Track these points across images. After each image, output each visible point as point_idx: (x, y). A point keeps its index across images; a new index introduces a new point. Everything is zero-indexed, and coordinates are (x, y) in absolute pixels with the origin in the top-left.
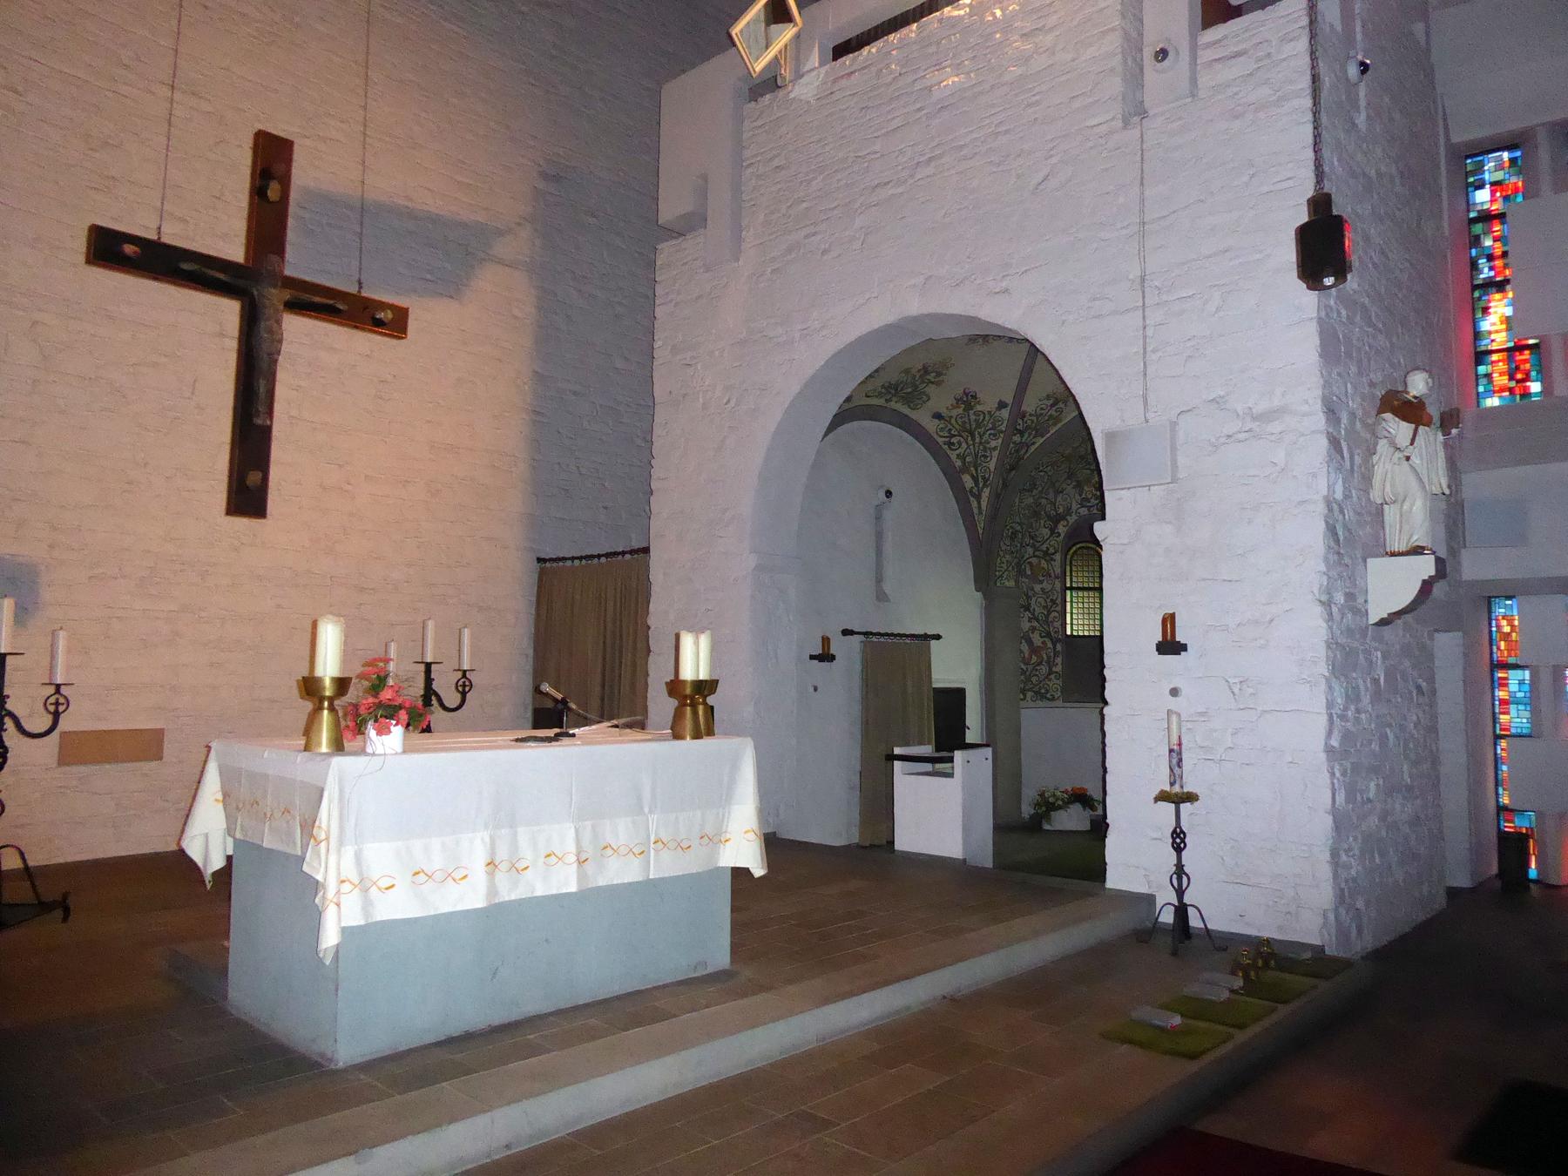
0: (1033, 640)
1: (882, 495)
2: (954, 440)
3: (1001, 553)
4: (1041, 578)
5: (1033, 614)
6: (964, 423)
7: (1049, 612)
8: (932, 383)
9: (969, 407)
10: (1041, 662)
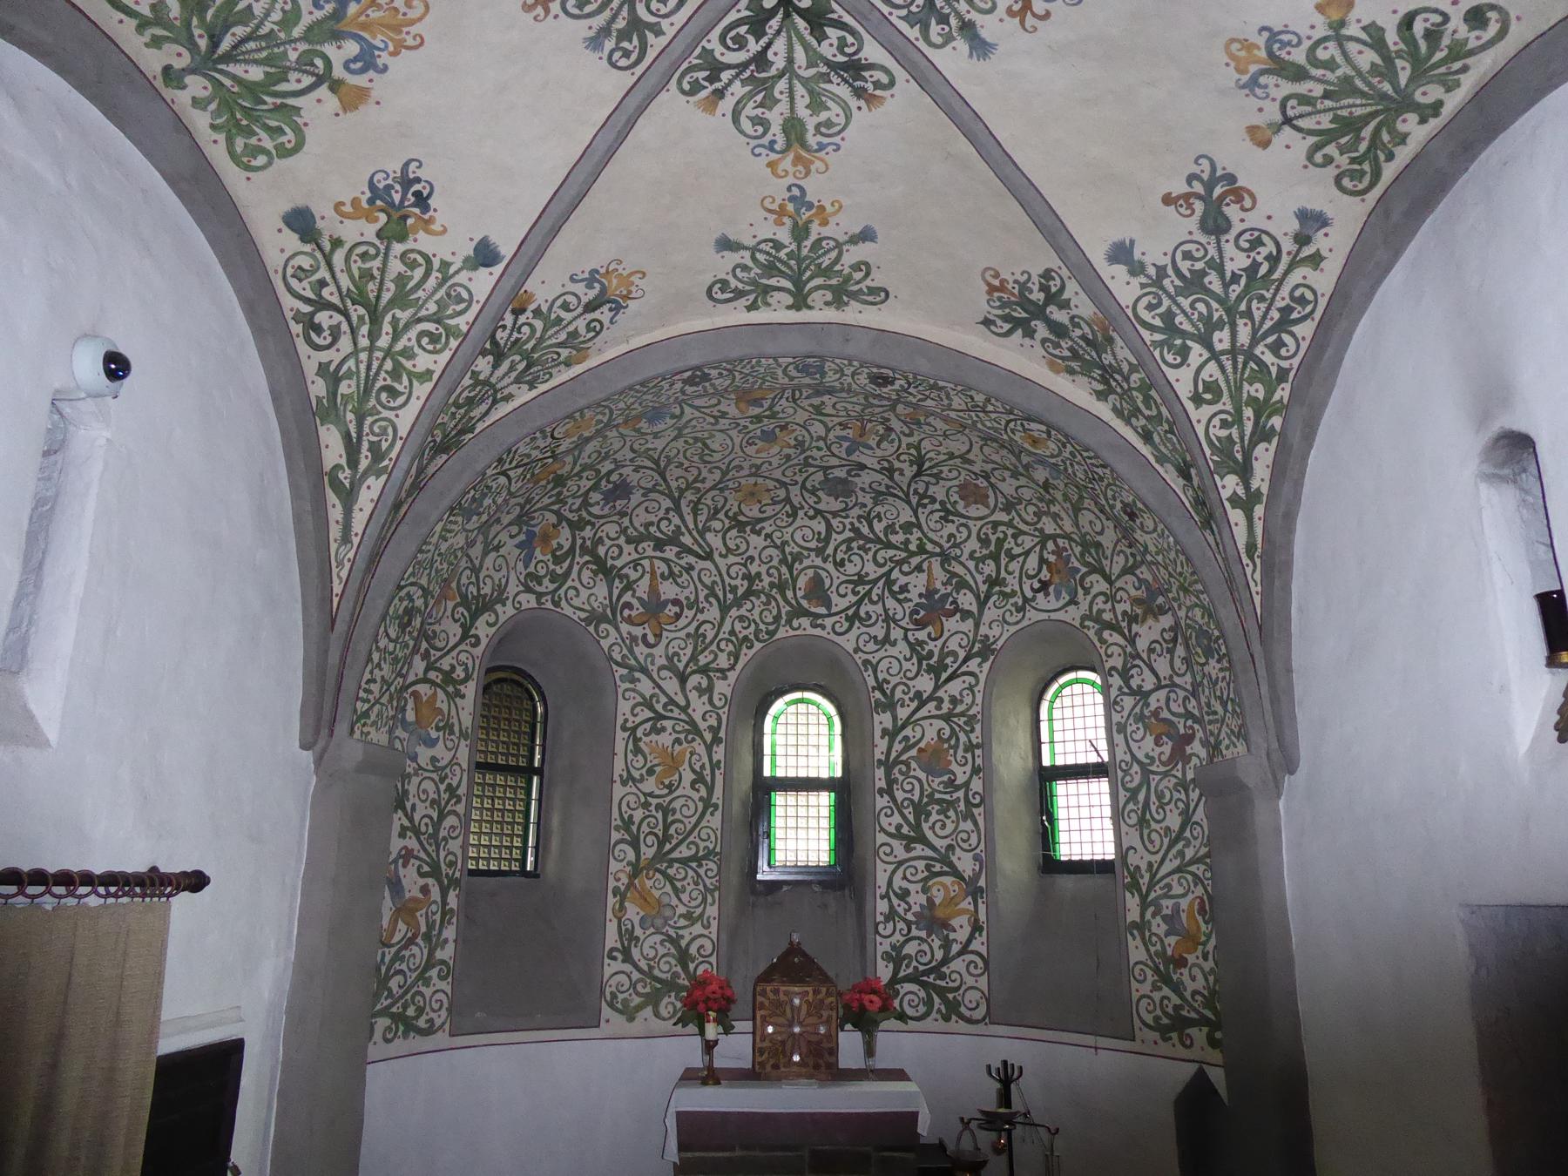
0: (404, 882)
1: (89, 367)
2: (323, 318)
3: (376, 656)
4: (434, 734)
5: (411, 820)
6: (367, 275)
7: (442, 816)
8: (336, 86)
9: (396, 230)
10: (415, 936)
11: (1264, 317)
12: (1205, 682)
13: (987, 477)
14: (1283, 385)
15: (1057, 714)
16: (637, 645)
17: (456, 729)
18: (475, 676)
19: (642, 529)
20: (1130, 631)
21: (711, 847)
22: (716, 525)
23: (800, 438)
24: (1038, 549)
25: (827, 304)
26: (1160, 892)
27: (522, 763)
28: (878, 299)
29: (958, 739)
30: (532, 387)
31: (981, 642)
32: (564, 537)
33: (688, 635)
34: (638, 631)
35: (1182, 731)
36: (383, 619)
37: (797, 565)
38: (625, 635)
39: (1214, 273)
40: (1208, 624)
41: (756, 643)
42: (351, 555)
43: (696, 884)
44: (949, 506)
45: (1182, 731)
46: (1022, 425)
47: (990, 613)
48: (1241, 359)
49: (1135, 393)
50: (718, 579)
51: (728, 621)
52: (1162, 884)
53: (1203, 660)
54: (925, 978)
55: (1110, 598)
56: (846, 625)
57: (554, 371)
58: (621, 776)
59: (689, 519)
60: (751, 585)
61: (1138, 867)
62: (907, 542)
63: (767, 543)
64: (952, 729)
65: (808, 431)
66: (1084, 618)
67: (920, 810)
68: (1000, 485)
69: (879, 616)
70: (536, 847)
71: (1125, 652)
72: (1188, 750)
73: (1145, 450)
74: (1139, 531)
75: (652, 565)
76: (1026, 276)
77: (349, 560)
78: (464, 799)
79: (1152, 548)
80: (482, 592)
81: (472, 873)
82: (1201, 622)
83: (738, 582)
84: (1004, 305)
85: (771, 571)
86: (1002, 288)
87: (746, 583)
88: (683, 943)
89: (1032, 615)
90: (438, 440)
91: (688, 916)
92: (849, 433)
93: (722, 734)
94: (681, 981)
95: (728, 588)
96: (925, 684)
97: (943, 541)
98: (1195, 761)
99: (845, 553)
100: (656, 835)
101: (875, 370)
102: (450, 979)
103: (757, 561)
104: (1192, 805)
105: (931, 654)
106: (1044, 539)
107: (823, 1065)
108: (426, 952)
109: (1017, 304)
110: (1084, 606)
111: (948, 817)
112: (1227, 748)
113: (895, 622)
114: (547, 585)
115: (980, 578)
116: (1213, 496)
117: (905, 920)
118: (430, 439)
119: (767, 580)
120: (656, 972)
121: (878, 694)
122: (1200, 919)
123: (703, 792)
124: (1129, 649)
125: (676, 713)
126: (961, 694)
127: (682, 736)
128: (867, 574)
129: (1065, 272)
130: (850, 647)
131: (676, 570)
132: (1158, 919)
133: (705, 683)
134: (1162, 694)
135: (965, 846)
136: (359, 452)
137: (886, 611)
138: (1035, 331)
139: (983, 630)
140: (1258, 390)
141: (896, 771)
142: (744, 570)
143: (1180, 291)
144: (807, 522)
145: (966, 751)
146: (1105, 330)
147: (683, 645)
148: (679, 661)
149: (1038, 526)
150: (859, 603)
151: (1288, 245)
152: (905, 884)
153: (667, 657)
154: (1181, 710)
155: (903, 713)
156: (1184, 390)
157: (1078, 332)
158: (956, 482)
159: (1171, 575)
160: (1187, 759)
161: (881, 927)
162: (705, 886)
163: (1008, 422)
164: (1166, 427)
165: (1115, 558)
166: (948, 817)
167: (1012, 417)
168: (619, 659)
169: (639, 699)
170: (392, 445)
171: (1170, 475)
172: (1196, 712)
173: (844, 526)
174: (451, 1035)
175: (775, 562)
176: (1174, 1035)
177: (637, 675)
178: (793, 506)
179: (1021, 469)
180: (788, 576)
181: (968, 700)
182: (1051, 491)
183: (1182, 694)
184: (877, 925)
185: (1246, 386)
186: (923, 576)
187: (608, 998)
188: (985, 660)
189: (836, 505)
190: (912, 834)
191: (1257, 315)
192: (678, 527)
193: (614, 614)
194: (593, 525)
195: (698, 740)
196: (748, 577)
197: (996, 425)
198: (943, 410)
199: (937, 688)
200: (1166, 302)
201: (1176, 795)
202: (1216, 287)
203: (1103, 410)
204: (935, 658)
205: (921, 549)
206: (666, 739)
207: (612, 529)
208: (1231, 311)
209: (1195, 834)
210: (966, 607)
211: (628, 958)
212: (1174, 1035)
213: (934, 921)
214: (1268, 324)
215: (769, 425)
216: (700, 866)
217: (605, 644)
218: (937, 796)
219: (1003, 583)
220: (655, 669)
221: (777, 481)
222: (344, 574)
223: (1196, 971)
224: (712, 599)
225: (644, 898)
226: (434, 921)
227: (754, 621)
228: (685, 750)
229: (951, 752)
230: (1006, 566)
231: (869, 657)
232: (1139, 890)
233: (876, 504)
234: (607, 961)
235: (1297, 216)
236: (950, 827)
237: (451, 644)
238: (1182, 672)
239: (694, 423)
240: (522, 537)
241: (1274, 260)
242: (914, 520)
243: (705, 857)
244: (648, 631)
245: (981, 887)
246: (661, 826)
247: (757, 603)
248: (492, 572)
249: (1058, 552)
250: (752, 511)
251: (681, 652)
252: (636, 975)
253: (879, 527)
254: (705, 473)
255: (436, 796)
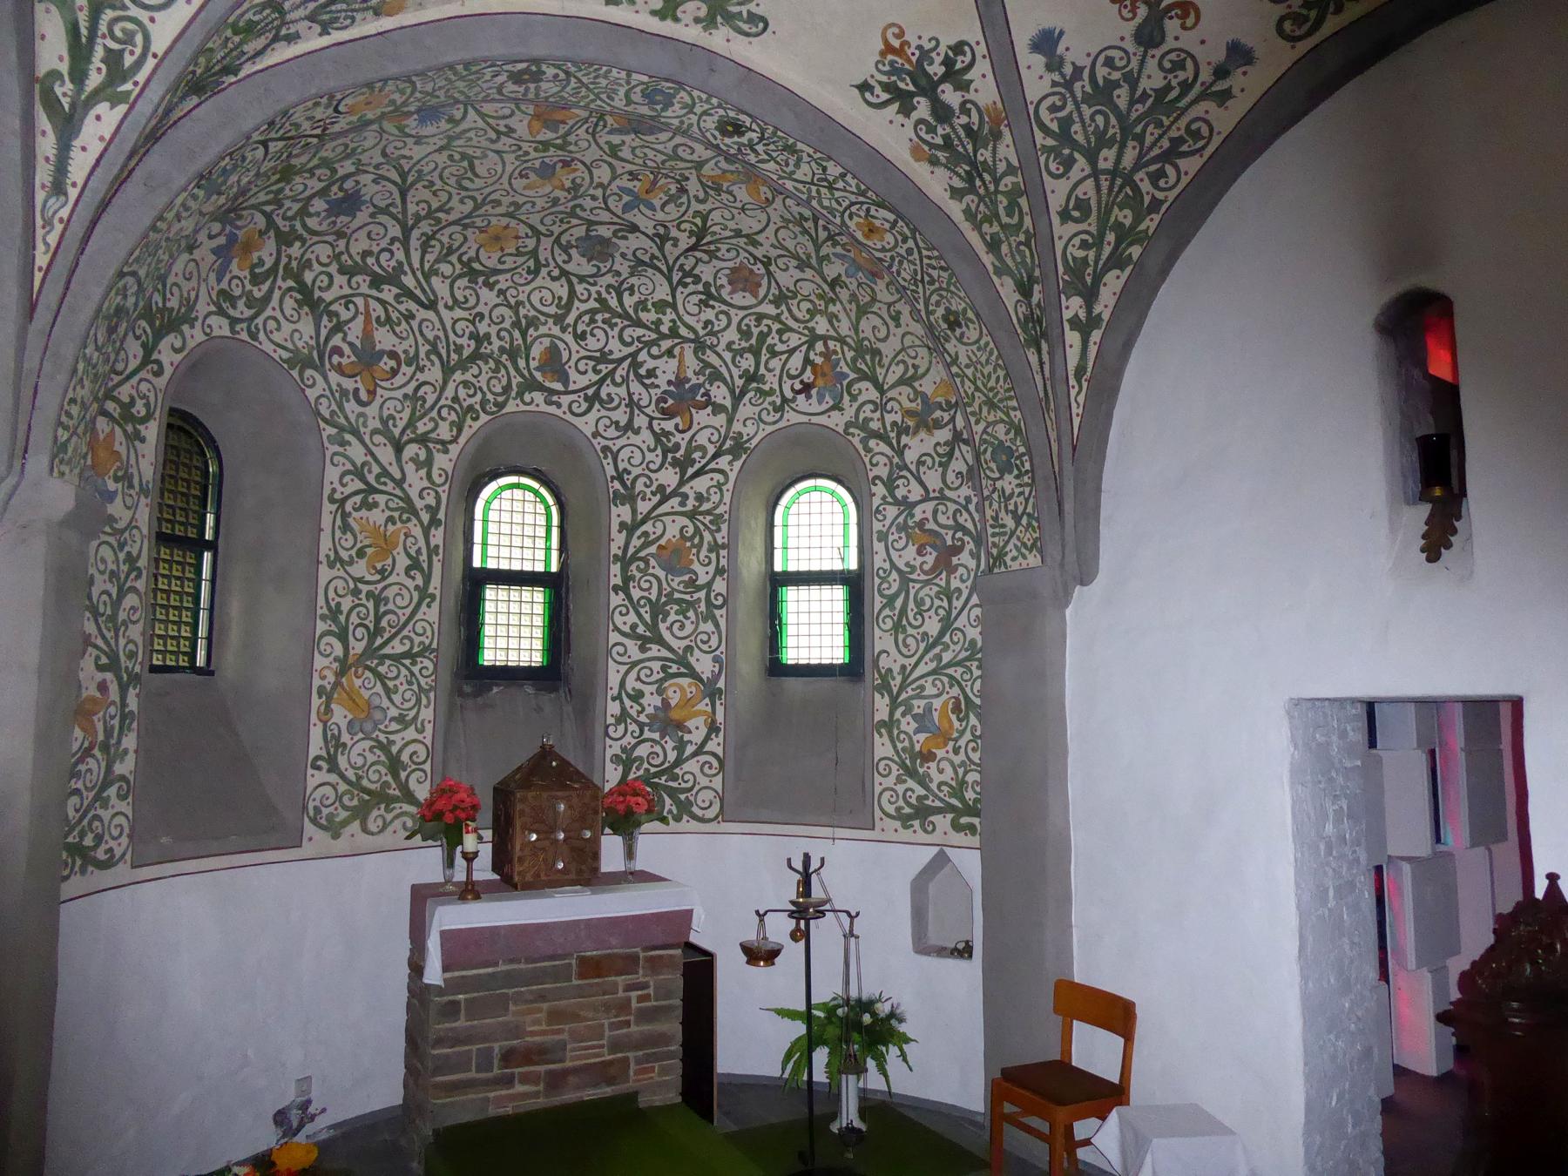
4: (111, 486)
10: (91, 747)
11: (1154, 144)
12: (995, 496)
13: (767, 263)
14: (1152, 216)
15: (792, 520)
16: (348, 401)
17: (136, 481)
18: (157, 415)
19: (358, 259)
20: (898, 442)
21: (427, 642)
22: (445, 269)
23: (578, 181)
24: (804, 348)
25: (697, 20)
26: (911, 693)
27: (192, 533)
28: (754, 30)
29: (702, 538)
30: (325, 32)
31: (733, 438)
32: (267, 252)
33: (406, 396)
34: (349, 384)
35: (949, 542)
36: (96, 317)
37: (531, 331)
38: (334, 387)
39: (1126, 86)
40: (1013, 441)
41: (482, 414)
42: (64, 213)
43: (410, 683)
44: (713, 290)
45: (949, 542)
46: (868, 210)
47: (745, 410)
48: (1119, 181)
49: (1000, 197)
50: (441, 334)
51: (451, 387)
52: (914, 686)
53: (997, 475)
54: (656, 780)
55: (880, 407)
56: (585, 406)
57: (359, 16)
58: (328, 556)
59: (415, 257)
60: (478, 348)
61: (890, 670)
62: (659, 322)
63: (499, 301)
64: (696, 528)
65: (591, 173)
66: (848, 425)
67: (658, 610)
68: (779, 275)
69: (622, 399)
70: (209, 639)
71: (891, 463)
72: (955, 560)
73: (988, 260)
74: (954, 341)
75: (367, 305)
76: (934, 43)
77: (61, 220)
78: (144, 573)
79: (963, 360)
80: (169, 305)
81: (154, 669)
82: (1002, 437)
83: (464, 341)
84: (895, 70)
85: (503, 333)
86: (899, 52)
87: (473, 343)
88: (394, 749)
89: (791, 417)
90: (199, 71)
91: (400, 719)
92: (636, 185)
93: (441, 515)
94: (391, 792)
95: (452, 347)
96: (669, 477)
97: (699, 327)
98: (961, 570)
99: (588, 325)
100: (366, 627)
101: (732, 114)
102: (130, 799)
103: (487, 320)
104: (954, 613)
105: (677, 447)
106: (813, 338)
107: (586, 874)
108: (103, 764)
109: (909, 73)
110: (849, 412)
111: (687, 618)
112: (1014, 559)
113: (640, 408)
114: (241, 310)
115: (736, 372)
116: (1055, 315)
117: (636, 721)
118: (191, 68)
119: (496, 343)
120: (365, 782)
121: (617, 485)
122: (953, 717)
123: (419, 581)
124: (896, 460)
125: (390, 487)
126: (708, 491)
127: (396, 514)
128: (611, 352)
129: (981, 50)
130: (588, 431)
131: (395, 315)
132: (909, 718)
133: (423, 455)
134: (929, 506)
135: (705, 647)
136: (88, 60)
137: (630, 395)
138: (915, 108)
139: (737, 427)
140: (1125, 217)
141: (633, 567)
142: (471, 328)
143: (1087, 99)
144: (548, 283)
145: (710, 550)
146: (997, 122)
147: (399, 408)
148: (395, 426)
149: (810, 325)
150: (601, 382)
151: (1206, 75)
152: (639, 686)
153: (381, 418)
154: (951, 522)
155: (643, 507)
156: (1056, 202)
157: (964, 120)
158: (731, 264)
159: (977, 389)
160: (952, 570)
161: (611, 729)
162: (419, 684)
163: (853, 204)
164: (1022, 238)
165: (893, 368)
166: (687, 618)
167: (861, 199)
168: (328, 416)
169: (349, 467)
170: (139, 64)
171: (1007, 291)
172: (969, 525)
173: (590, 295)
174: (133, 867)
175: (507, 324)
176: (916, 823)
177: (348, 437)
178: (537, 261)
179: (814, 261)
180: (520, 341)
181: (715, 498)
182: (838, 289)
183: (952, 507)
184: (607, 727)
185: (1116, 209)
186: (674, 363)
187: (311, 813)
188: (736, 458)
189: (587, 269)
190: (648, 634)
191: (1149, 140)
192: (400, 264)
193: (321, 357)
194: (304, 241)
195: (415, 521)
196: (475, 336)
197: (835, 205)
198: (781, 178)
199: (682, 483)
200: (1070, 106)
201: (937, 602)
202: (1122, 103)
203: (955, 209)
204: (682, 452)
205: (674, 332)
206: (378, 516)
207: (324, 252)
208: (1126, 130)
209: (955, 639)
210: (719, 400)
211: (334, 768)
212: (916, 823)
213: (668, 723)
214: (1156, 151)
215: (553, 155)
216: (414, 663)
217: (312, 394)
218: (677, 595)
219: (761, 379)
220: (368, 430)
221: (531, 227)
222: (53, 239)
223: (945, 764)
224: (433, 357)
225: (352, 700)
226: (113, 727)
227: (480, 388)
228: (400, 530)
229: (694, 551)
230: (767, 363)
231: (610, 443)
232: (890, 692)
233: (632, 274)
234: (310, 771)
235: (1228, 49)
236: (689, 628)
237: (131, 368)
238: (955, 485)
239: (471, 134)
240: (222, 240)
241: (1186, 87)
242: (670, 299)
243: (419, 654)
244: (360, 385)
245: (720, 689)
246: (372, 617)
247: (485, 368)
248: (180, 280)
249: (827, 355)
250: (490, 259)
251: (397, 416)
252: (343, 787)
253: (628, 301)
254: (455, 202)
255: (114, 568)
